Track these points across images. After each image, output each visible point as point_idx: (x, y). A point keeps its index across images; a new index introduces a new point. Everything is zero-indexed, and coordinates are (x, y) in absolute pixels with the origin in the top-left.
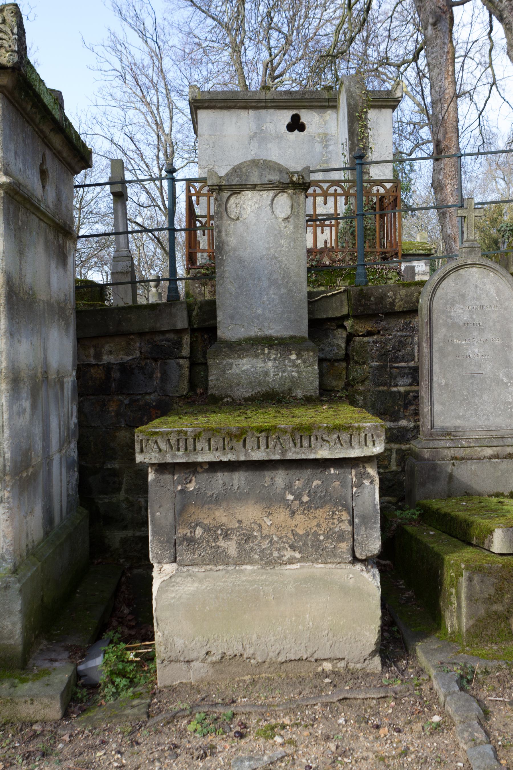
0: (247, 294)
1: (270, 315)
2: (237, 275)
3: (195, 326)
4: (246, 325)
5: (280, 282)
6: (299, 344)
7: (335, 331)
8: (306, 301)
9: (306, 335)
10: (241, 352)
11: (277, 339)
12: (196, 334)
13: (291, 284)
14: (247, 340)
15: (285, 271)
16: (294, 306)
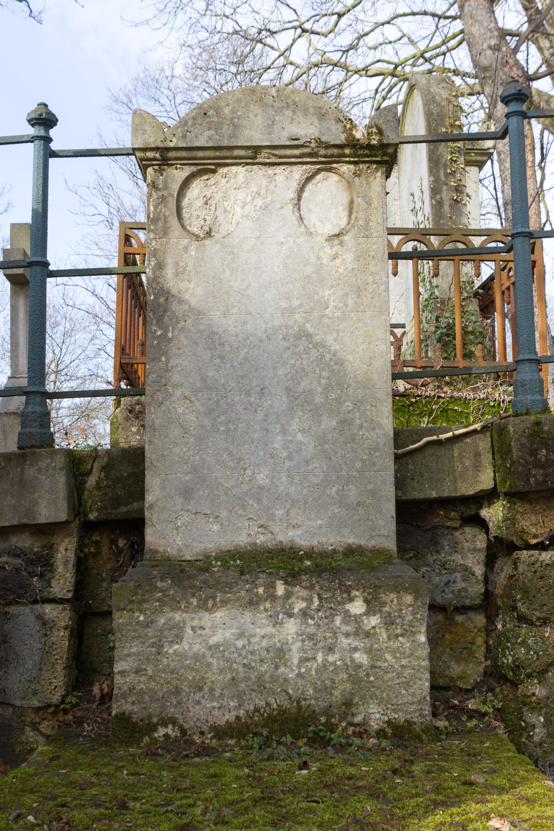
0: (228, 431)
1: (292, 489)
2: (204, 379)
3: (93, 516)
4: (224, 514)
5: (318, 399)
6: (373, 569)
7: (457, 534)
8: (389, 450)
9: (391, 545)
10: (209, 592)
11: (310, 554)
12: (96, 538)
13: (349, 405)
14: (227, 557)
15: (332, 371)
16: (358, 465)
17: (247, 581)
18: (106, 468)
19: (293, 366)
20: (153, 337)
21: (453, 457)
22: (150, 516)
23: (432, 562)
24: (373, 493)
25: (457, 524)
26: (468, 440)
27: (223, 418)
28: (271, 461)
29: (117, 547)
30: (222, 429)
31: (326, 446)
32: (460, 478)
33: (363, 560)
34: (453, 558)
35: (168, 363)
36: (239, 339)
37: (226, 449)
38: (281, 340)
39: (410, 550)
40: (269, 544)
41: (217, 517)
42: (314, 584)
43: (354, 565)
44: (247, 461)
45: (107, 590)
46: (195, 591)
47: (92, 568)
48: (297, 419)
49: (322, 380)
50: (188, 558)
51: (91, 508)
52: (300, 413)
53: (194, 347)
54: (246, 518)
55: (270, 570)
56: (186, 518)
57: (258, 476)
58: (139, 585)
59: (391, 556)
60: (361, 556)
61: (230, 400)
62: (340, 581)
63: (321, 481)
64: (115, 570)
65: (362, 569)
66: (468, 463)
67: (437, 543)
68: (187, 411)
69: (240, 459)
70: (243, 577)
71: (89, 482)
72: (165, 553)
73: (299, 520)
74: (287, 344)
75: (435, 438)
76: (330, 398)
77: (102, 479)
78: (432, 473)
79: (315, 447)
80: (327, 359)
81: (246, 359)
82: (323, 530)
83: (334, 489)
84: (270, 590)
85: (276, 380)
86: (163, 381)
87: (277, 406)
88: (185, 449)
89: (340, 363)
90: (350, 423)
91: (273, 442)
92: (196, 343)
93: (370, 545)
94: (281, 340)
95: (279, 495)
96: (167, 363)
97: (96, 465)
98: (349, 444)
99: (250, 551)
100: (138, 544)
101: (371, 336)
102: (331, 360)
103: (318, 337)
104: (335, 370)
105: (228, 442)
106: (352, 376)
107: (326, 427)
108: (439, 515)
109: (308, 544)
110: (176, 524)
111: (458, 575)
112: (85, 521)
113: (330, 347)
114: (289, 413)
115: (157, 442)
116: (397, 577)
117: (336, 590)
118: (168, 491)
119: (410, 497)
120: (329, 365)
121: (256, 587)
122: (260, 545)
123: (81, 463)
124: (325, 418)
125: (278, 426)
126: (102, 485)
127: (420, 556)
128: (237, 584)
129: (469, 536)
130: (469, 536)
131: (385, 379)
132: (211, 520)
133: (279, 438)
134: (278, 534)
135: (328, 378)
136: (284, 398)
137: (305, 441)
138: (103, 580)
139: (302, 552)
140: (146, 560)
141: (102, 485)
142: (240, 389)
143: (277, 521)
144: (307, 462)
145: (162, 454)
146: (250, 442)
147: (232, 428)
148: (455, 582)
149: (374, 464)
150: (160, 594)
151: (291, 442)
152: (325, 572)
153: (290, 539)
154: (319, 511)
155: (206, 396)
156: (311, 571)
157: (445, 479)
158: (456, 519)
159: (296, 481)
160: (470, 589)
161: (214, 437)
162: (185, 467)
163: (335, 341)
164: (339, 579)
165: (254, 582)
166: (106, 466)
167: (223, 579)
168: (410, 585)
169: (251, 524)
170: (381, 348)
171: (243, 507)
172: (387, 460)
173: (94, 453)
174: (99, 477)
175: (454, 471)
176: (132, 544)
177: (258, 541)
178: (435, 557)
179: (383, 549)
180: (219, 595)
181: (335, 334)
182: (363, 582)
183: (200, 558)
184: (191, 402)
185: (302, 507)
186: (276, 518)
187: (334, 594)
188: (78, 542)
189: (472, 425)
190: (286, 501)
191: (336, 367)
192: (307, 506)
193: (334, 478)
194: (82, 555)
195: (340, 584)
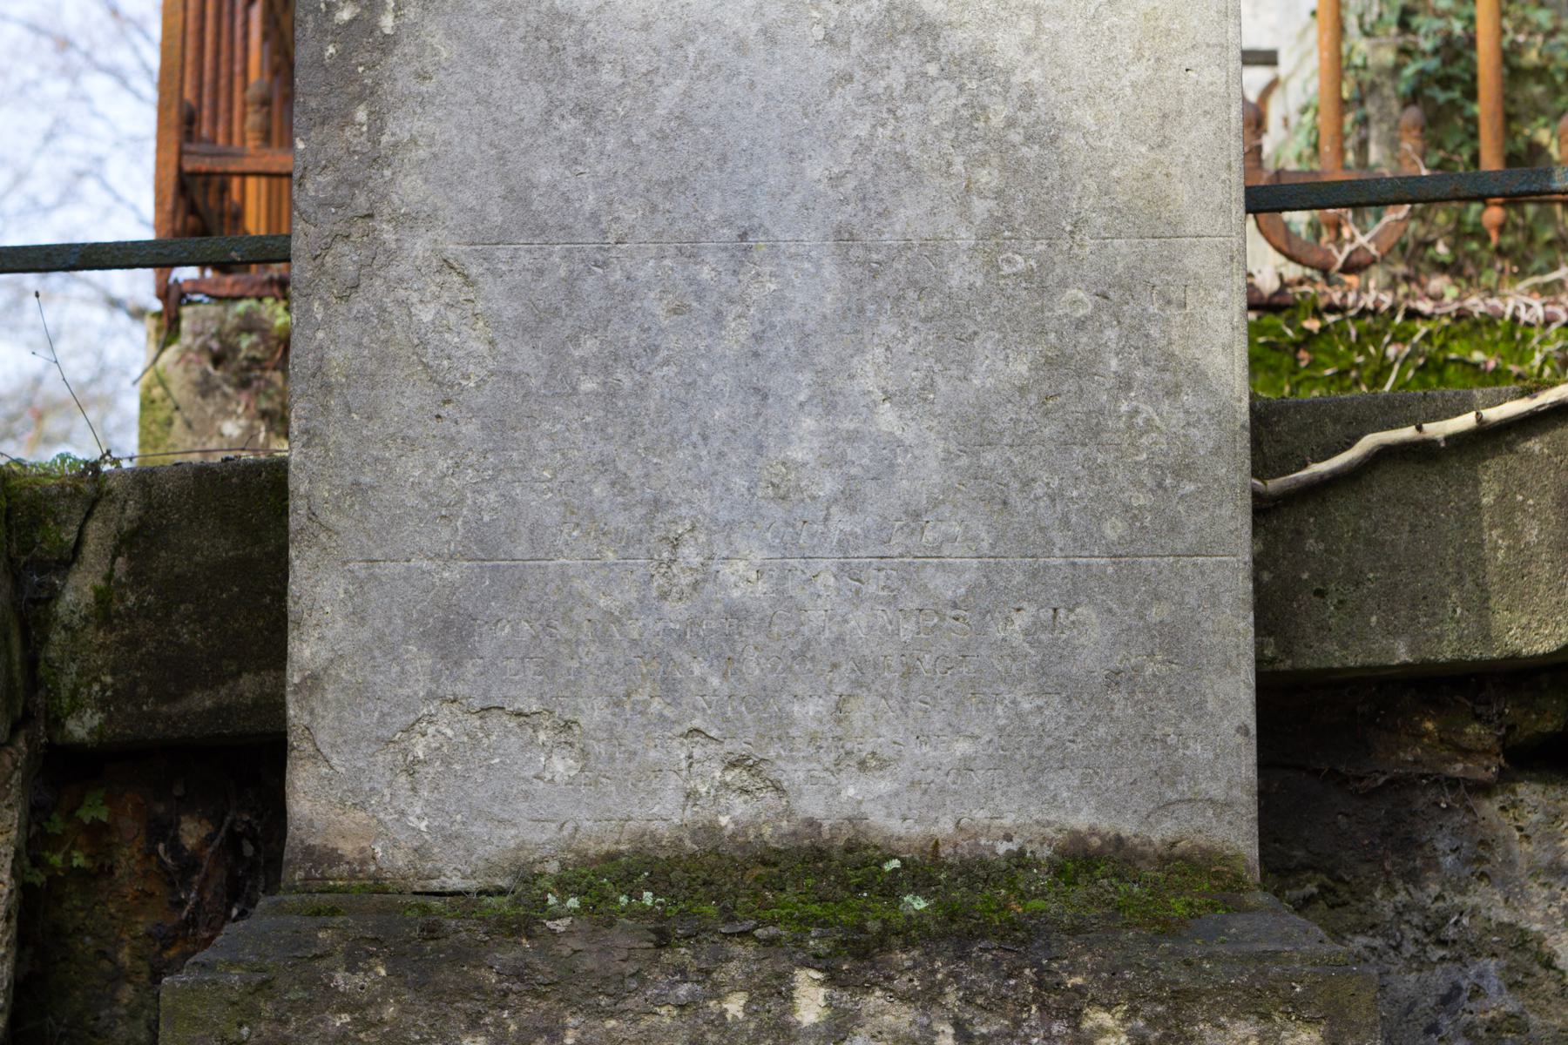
0: (610, 394)
1: (858, 621)
2: (517, 196)
3: (82, 727)
4: (594, 713)
5: (961, 275)
6: (1167, 928)
7: (1489, 808)
8: (1232, 475)
9: (1238, 837)
10: (534, 1009)
11: (925, 868)
12: (94, 811)
13: (1077, 299)
14: (604, 879)
15: (1014, 168)
16: (1113, 529)
17: (682, 971)
18: (135, 542)
19: (864, 147)
20: (321, 31)
21: (1476, 507)
22: (307, 719)
23: (1389, 913)
24: (1171, 640)
25: (1486, 769)
26: (1535, 445)
27: (590, 345)
28: (776, 511)
29: (175, 848)
30: (588, 385)
31: (989, 457)
32: (1503, 590)
33: (1130, 895)
34: (1471, 900)
35: (381, 131)
36: (655, 39)
37: (604, 464)
38: (818, 44)
39: (1305, 867)
40: (767, 831)
41: (568, 726)
42: (942, 984)
43: (1095, 911)
44: (684, 510)
45: (134, 1016)
46: (480, 1006)
47: (79, 930)
48: (879, 351)
49: (976, 201)
50: (455, 882)
51: (74, 693)
52: (890, 329)
53: (482, 69)
54: (678, 730)
55: (772, 930)
56: (446, 727)
57: (726, 570)
58: (264, 982)
59: (1238, 878)
60: (1120, 877)
61: (618, 275)
62: (1042, 970)
63: (971, 591)
64: (167, 942)
65: (1127, 926)
66: (1532, 534)
67: (1409, 844)
68: (452, 317)
69: (657, 505)
70: (666, 957)
71: (69, 597)
72: (363, 862)
73: (882, 738)
74: (840, 63)
75: (1408, 433)
76: (1006, 269)
77: (119, 583)
78: (1396, 568)
79: (948, 458)
80: (997, 121)
81: (683, 119)
82: (978, 779)
83: (1021, 621)
84: (770, 1004)
85: (797, 198)
86: (362, 201)
87: (801, 299)
88: (442, 465)
89: (1047, 136)
90: (1086, 369)
91: (785, 439)
92: (488, 56)
93: (1156, 838)
94: (818, 44)
95: (807, 644)
96: (376, 130)
97: (95, 529)
98: (1077, 450)
99: (692, 856)
100: (254, 841)
101: (1168, 33)
102: (1011, 123)
103: (960, 35)
104: (1026, 163)
105: (609, 439)
106: (1093, 187)
107: (990, 382)
108: (1419, 735)
109: (917, 830)
110: (405, 752)
111: (1492, 964)
112: (50, 746)
113: (1008, 72)
114: (848, 327)
115: (334, 434)
116: (1260, 958)
117: (1025, 1006)
118: (378, 624)
119: (1309, 663)
120: (1000, 143)
121: (717, 993)
122: (733, 836)
123: (36, 522)
124: (985, 348)
125: (806, 377)
126: (117, 606)
127: (1343, 891)
128: (643, 981)
129: (1534, 818)
130: (1534, 818)
131: (1219, 198)
132: (542, 736)
133: (808, 423)
134: (800, 794)
135: (999, 194)
136: (829, 270)
137: (909, 437)
138: (120, 976)
139: (896, 863)
140: (292, 889)
141: (117, 606)
142: (659, 234)
143: (799, 743)
144: (917, 516)
145: (357, 483)
146: (695, 437)
147: (627, 383)
148: (1477, 992)
149: (1174, 527)
150: (346, 1018)
151: (853, 437)
152: (983, 937)
153: (848, 811)
154: (960, 703)
155: (525, 260)
156: (927, 936)
157: (1445, 595)
158: (1486, 752)
159: (872, 588)
160: (1534, 1019)
161: (557, 419)
162: (445, 534)
163: (1028, 51)
164: (1037, 964)
165: (708, 973)
166: (135, 533)
167: (590, 963)
168: (1311, 988)
169: (697, 753)
170: (1207, 77)
171: (669, 688)
172: (1226, 510)
173: (89, 486)
174: (108, 578)
175: (1481, 561)
176: (233, 841)
177: (724, 820)
178: (1402, 897)
179: (1208, 855)
180: (571, 1021)
181: (1027, 26)
182: (1128, 975)
183: (499, 882)
184: (468, 281)
185: (895, 689)
186: (793, 732)
187: (1017, 1023)
188: (26, 826)
189: (1552, 385)
190: (835, 666)
191: (1030, 152)
192: (916, 685)
193: (1019, 578)
194: (39, 878)
195: (1040, 984)
